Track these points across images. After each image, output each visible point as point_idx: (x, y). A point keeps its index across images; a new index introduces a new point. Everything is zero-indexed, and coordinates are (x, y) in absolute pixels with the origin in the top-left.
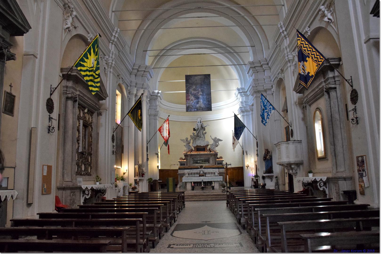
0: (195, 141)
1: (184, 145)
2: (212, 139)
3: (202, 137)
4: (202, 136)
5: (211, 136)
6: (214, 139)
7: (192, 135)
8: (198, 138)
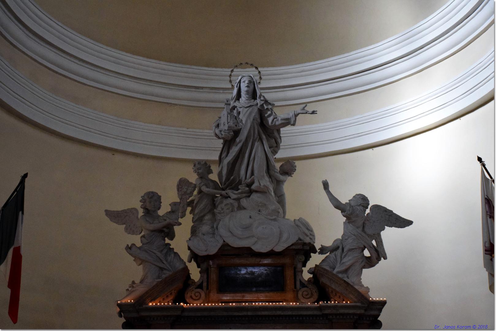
0: (207, 217)
1: (129, 248)
2: (338, 205)
3: (263, 192)
4: (266, 182)
5: (326, 185)
6: (349, 204)
7: (193, 178)
8: (233, 195)
